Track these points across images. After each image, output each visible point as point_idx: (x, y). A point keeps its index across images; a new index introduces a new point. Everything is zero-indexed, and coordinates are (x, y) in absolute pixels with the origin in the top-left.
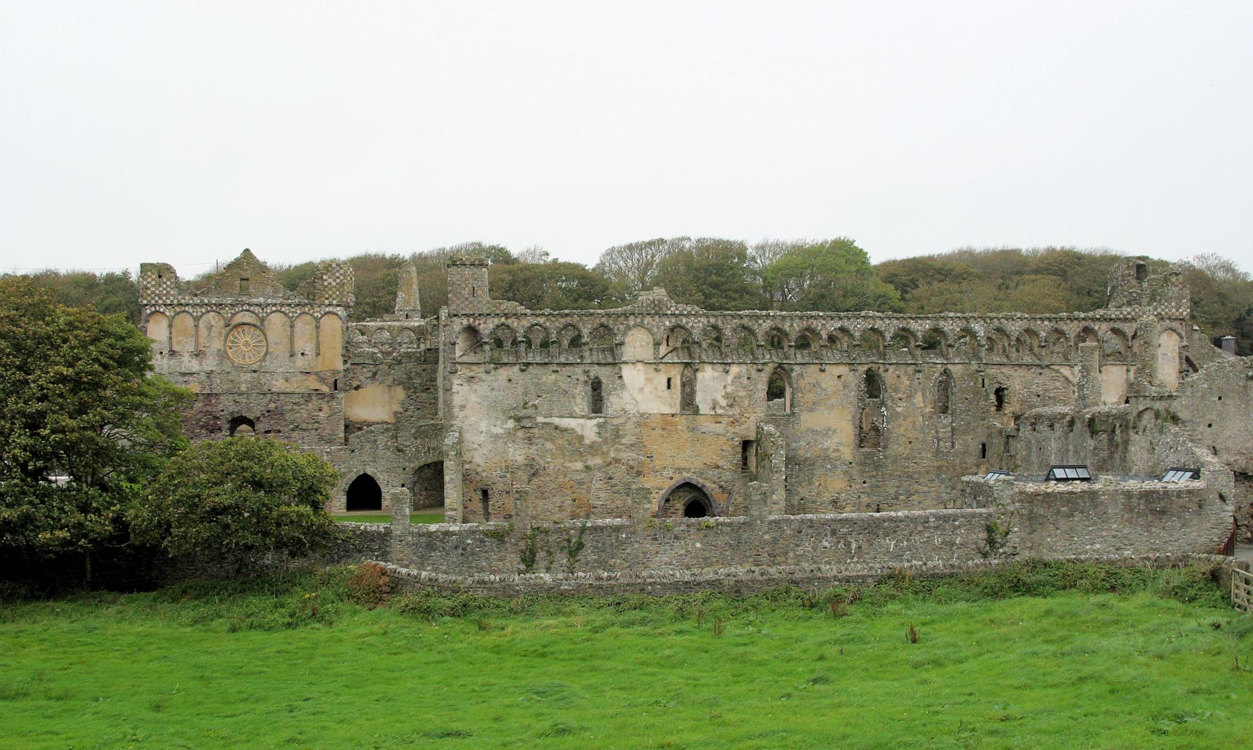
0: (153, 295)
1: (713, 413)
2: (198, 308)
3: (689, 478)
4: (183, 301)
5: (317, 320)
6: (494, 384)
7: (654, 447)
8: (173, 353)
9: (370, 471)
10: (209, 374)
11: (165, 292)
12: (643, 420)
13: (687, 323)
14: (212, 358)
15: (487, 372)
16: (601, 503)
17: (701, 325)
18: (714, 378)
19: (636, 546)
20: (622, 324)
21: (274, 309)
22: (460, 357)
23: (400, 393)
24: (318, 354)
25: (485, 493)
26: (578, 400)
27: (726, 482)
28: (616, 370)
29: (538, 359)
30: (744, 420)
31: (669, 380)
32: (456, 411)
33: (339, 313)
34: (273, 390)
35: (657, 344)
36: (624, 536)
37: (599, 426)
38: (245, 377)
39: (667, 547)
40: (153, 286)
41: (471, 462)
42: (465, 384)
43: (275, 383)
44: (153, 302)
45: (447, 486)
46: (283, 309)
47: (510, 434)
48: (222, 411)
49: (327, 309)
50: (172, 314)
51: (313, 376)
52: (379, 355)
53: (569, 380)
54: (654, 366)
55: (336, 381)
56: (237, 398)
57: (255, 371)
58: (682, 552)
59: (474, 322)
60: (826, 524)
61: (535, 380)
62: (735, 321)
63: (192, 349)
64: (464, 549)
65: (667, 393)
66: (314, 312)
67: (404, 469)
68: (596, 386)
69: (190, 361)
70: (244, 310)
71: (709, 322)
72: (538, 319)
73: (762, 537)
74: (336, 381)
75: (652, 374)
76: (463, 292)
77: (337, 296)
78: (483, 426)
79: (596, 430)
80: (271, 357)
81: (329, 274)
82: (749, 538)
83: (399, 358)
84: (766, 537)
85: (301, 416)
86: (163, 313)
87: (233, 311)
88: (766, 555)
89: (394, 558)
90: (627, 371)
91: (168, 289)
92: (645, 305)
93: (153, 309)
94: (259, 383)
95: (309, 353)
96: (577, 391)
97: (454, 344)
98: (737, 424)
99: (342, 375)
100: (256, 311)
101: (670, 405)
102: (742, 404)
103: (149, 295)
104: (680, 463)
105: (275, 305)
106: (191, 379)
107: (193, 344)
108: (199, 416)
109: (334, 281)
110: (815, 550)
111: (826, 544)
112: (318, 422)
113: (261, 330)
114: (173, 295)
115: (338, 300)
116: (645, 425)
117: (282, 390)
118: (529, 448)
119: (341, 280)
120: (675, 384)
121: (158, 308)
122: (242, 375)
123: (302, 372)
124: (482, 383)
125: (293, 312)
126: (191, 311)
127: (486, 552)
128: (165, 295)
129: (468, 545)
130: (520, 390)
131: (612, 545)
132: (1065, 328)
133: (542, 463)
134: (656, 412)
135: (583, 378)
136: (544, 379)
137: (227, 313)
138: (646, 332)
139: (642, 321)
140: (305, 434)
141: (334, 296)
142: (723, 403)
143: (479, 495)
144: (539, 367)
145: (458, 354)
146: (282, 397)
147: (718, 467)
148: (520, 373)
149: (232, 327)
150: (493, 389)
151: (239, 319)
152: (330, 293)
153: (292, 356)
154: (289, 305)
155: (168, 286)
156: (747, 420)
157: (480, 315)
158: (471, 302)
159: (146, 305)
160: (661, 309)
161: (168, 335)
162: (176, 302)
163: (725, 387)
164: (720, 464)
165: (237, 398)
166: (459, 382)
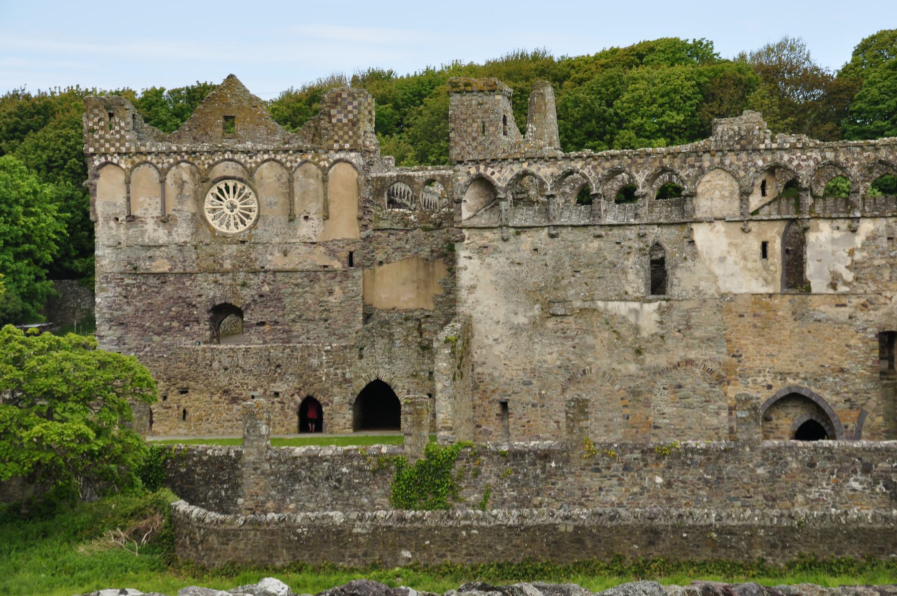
0: (102, 141)
1: (831, 291)
2: (164, 157)
3: (797, 387)
4: (143, 149)
5: (325, 171)
6: (513, 256)
7: (743, 342)
8: (132, 219)
10: (181, 247)
11: (118, 136)
12: (726, 301)
13: (791, 161)
14: (185, 225)
15: (505, 240)
16: (667, 421)
17: (812, 163)
18: (833, 241)
19: (570, 479)
20: (693, 166)
21: (266, 157)
22: (469, 218)
24: (326, 217)
25: (504, 405)
26: (631, 276)
27: (856, 394)
28: (685, 232)
29: (575, 220)
30: (882, 300)
31: (764, 245)
32: (463, 294)
33: (354, 161)
34: (267, 267)
35: (745, 194)
36: (553, 465)
37: (661, 311)
38: (230, 251)
39: (615, 481)
40: (102, 128)
41: (484, 363)
42: (475, 256)
43: (270, 258)
44: (103, 150)
46: (278, 157)
47: (535, 325)
48: (200, 296)
50: (130, 166)
51: (322, 249)
52: (412, 217)
53: (618, 247)
54: (741, 225)
55: (351, 254)
56: (219, 278)
57: (243, 242)
58: (636, 489)
59: (485, 170)
60: (855, 456)
61: (571, 249)
62: (866, 154)
63: (157, 213)
64: (339, 481)
65: (759, 264)
66: (319, 161)
69: (155, 230)
70: (225, 160)
71: (824, 158)
72: (573, 164)
73: (753, 471)
74: (351, 254)
75: (741, 238)
76: (469, 130)
77: (350, 137)
78: (500, 313)
79: (656, 317)
81: (339, 108)
82: (734, 473)
83: (438, 221)
84: (760, 471)
85: (305, 303)
86: (117, 165)
87: (211, 162)
88: (760, 497)
89: (246, 491)
90: (700, 233)
91: (123, 132)
93: (103, 160)
94: (248, 258)
95: (314, 217)
96: (629, 263)
97: (459, 201)
98: (871, 307)
99: (358, 245)
100: (243, 161)
101: (766, 280)
102: (878, 278)
103: (97, 141)
104: (781, 364)
105: (266, 152)
106: (158, 253)
107: (159, 206)
109: (346, 116)
110: (837, 493)
111: (856, 485)
112: (328, 310)
113: (250, 186)
114: (130, 141)
115: (351, 141)
116: (730, 311)
117: (280, 266)
118: (563, 344)
119: (355, 116)
120: (774, 249)
121: (109, 158)
123: (305, 243)
125: (291, 162)
126: (154, 161)
127: (368, 485)
128: (118, 140)
129: (343, 474)
130: (551, 263)
131: (536, 477)
133: (582, 365)
134: (743, 291)
136: (583, 247)
137: (204, 161)
138: (730, 177)
139: (722, 162)
140: (311, 326)
141: (346, 137)
142: (849, 276)
143: (497, 409)
144: (576, 231)
145: (466, 214)
146: (279, 277)
147: (842, 371)
148: (549, 240)
149: (204, 180)
150: (512, 263)
151: (220, 170)
152: (341, 133)
153: (291, 220)
154: (286, 151)
155: (121, 128)
156: (888, 301)
157: (493, 160)
158: (481, 144)
159: (93, 154)
160: (750, 142)
161: (125, 194)
162: (133, 150)
163: (851, 253)
164: (846, 366)
165: (219, 278)
166: (467, 253)
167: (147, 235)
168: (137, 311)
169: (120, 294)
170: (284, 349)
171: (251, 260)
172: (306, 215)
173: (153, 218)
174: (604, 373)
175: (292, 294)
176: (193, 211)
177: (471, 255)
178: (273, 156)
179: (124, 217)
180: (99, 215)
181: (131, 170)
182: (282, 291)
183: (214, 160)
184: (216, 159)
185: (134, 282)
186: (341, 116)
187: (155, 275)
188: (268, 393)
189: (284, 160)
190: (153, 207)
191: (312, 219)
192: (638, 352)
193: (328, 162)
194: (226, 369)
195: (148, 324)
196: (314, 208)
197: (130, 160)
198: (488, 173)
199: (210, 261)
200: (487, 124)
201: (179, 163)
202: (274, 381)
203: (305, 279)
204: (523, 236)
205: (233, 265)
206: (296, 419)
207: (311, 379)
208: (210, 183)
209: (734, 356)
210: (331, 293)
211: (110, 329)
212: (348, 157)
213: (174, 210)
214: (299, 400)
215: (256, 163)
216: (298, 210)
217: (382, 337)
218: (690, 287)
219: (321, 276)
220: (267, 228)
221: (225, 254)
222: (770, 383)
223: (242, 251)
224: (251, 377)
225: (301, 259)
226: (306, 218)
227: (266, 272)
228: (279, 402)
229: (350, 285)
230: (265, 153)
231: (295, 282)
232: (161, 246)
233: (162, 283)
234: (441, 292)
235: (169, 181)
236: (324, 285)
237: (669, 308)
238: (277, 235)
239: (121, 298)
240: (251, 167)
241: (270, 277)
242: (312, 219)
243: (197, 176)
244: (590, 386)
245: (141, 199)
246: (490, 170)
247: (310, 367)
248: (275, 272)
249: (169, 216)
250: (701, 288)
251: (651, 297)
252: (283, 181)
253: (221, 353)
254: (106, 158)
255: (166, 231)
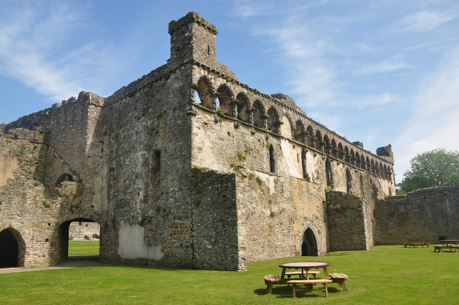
9: (16, 225)
23: (14, 164)
31: (298, 155)
32: (195, 152)
42: (202, 128)
45: (239, 222)
53: (259, 142)
67: (49, 224)
68: (271, 149)
72: (244, 89)
92: (289, 102)
124: (213, 131)
132: (378, 161)
135: (266, 143)
136: (247, 138)
138: (288, 121)
157: (213, 71)
174: (260, 215)
177: (200, 126)
192: (270, 202)
198: (210, 77)
200: (210, 48)
204: (223, 123)
209: (294, 208)
217: (17, 196)
218: (282, 171)
222: (303, 222)
234: (13, 178)
237: (277, 180)
244: (255, 222)
246: (210, 77)
250: (285, 172)
251: (271, 173)
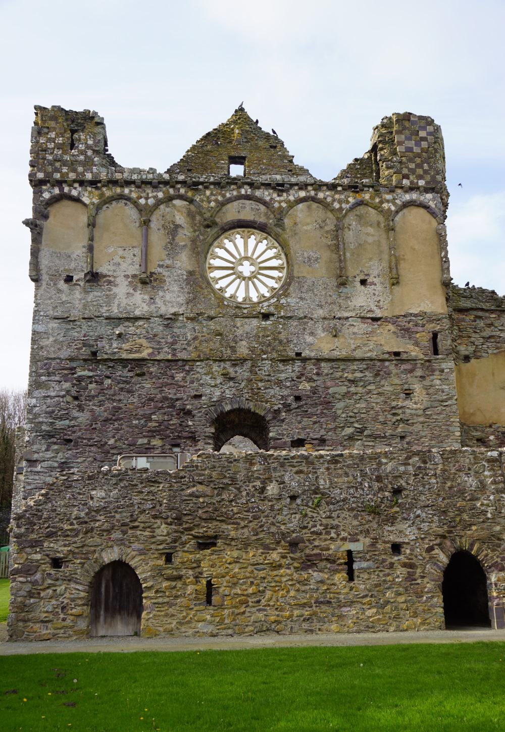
0: (58, 164)
2: (149, 190)
5: (389, 216)
8: (94, 277)
10: (170, 320)
14: (176, 288)
21: (302, 194)
33: (432, 204)
38: (247, 328)
40: (59, 146)
44: (57, 176)
46: (321, 195)
48: (198, 397)
49: (407, 197)
50: (96, 201)
51: (391, 327)
55: (435, 336)
57: (266, 316)
66: (381, 202)
70: (240, 197)
74: (435, 336)
80: (300, 288)
85: (369, 409)
87: (220, 198)
91: (90, 153)
93: (56, 191)
94: (275, 339)
95: (376, 280)
100: (268, 199)
106: (132, 330)
107: (137, 259)
108: (147, 410)
115: (428, 178)
117: (326, 354)
121: (66, 189)
122: (239, 322)
125: (340, 202)
126: (134, 195)
151: (232, 212)
152: (412, 166)
153: (343, 283)
161: (85, 242)
165: (231, 370)
167: (116, 302)
168: (94, 419)
169: (68, 392)
170: (408, 458)
171: (281, 342)
172: (363, 277)
173: (126, 276)
175: (348, 395)
176: (190, 268)
178: (313, 193)
179: (82, 275)
180: (43, 272)
181: (98, 208)
182: (331, 391)
183: (224, 196)
184: (228, 195)
185: (91, 374)
186: (411, 144)
187: (124, 362)
188: (380, 546)
189: (329, 199)
190: (129, 261)
191: (373, 284)
193: (395, 204)
194: (293, 498)
195: (111, 442)
196: (376, 269)
197: (97, 192)
199: (216, 343)
201: (169, 199)
202: (392, 520)
203: (367, 373)
205: (252, 350)
206: (438, 600)
207: (465, 516)
208: (215, 230)
210: (408, 394)
211: (47, 450)
212: (422, 198)
213: (160, 266)
214: (444, 559)
215: (288, 202)
216: (352, 270)
219: (392, 367)
220: (303, 295)
221: (239, 332)
223: (265, 329)
224: (346, 514)
225: (359, 342)
226: (363, 282)
227: (305, 360)
228: (405, 565)
229: (438, 382)
230: (301, 189)
231: (350, 376)
232: (137, 319)
233: (138, 375)
235: (154, 225)
236: (397, 381)
238: (321, 306)
239: (69, 398)
240: (280, 207)
241: (310, 366)
242: (373, 284)
243: (198, 218)
245: (111, 250)
247: (462, 492)
248: (319, 360)
249: (152, 273)
252: (327, 228)
253: (282, 465)
254: (61, 189)
255: (147, 297)
